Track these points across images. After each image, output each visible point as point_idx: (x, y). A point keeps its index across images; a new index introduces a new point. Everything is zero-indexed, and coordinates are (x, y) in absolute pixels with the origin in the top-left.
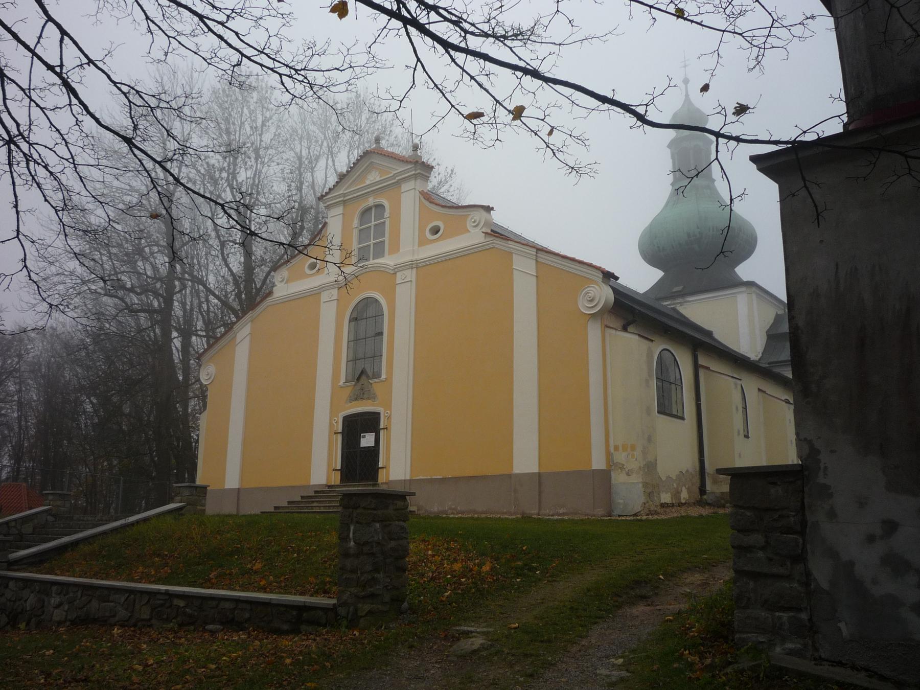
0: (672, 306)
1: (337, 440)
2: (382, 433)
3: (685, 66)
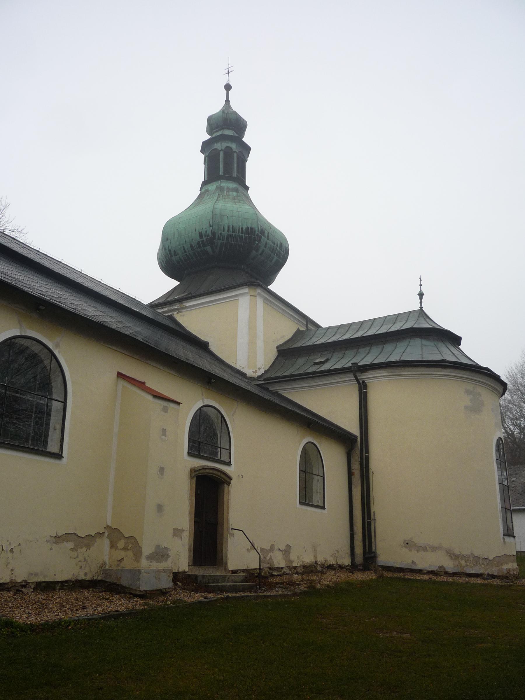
0: (169, 314)
3: (228, 73)
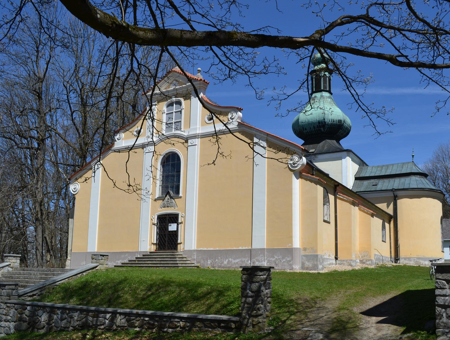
1: (154, 227)
2: (180, 225)
